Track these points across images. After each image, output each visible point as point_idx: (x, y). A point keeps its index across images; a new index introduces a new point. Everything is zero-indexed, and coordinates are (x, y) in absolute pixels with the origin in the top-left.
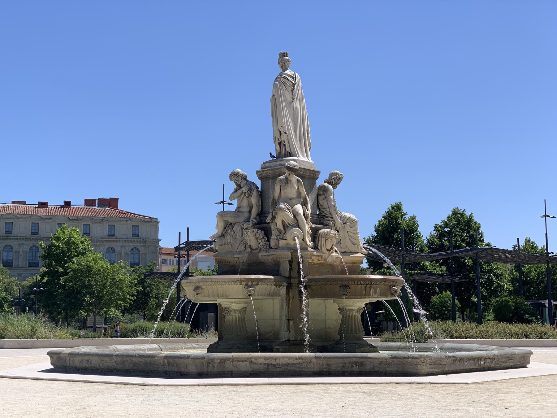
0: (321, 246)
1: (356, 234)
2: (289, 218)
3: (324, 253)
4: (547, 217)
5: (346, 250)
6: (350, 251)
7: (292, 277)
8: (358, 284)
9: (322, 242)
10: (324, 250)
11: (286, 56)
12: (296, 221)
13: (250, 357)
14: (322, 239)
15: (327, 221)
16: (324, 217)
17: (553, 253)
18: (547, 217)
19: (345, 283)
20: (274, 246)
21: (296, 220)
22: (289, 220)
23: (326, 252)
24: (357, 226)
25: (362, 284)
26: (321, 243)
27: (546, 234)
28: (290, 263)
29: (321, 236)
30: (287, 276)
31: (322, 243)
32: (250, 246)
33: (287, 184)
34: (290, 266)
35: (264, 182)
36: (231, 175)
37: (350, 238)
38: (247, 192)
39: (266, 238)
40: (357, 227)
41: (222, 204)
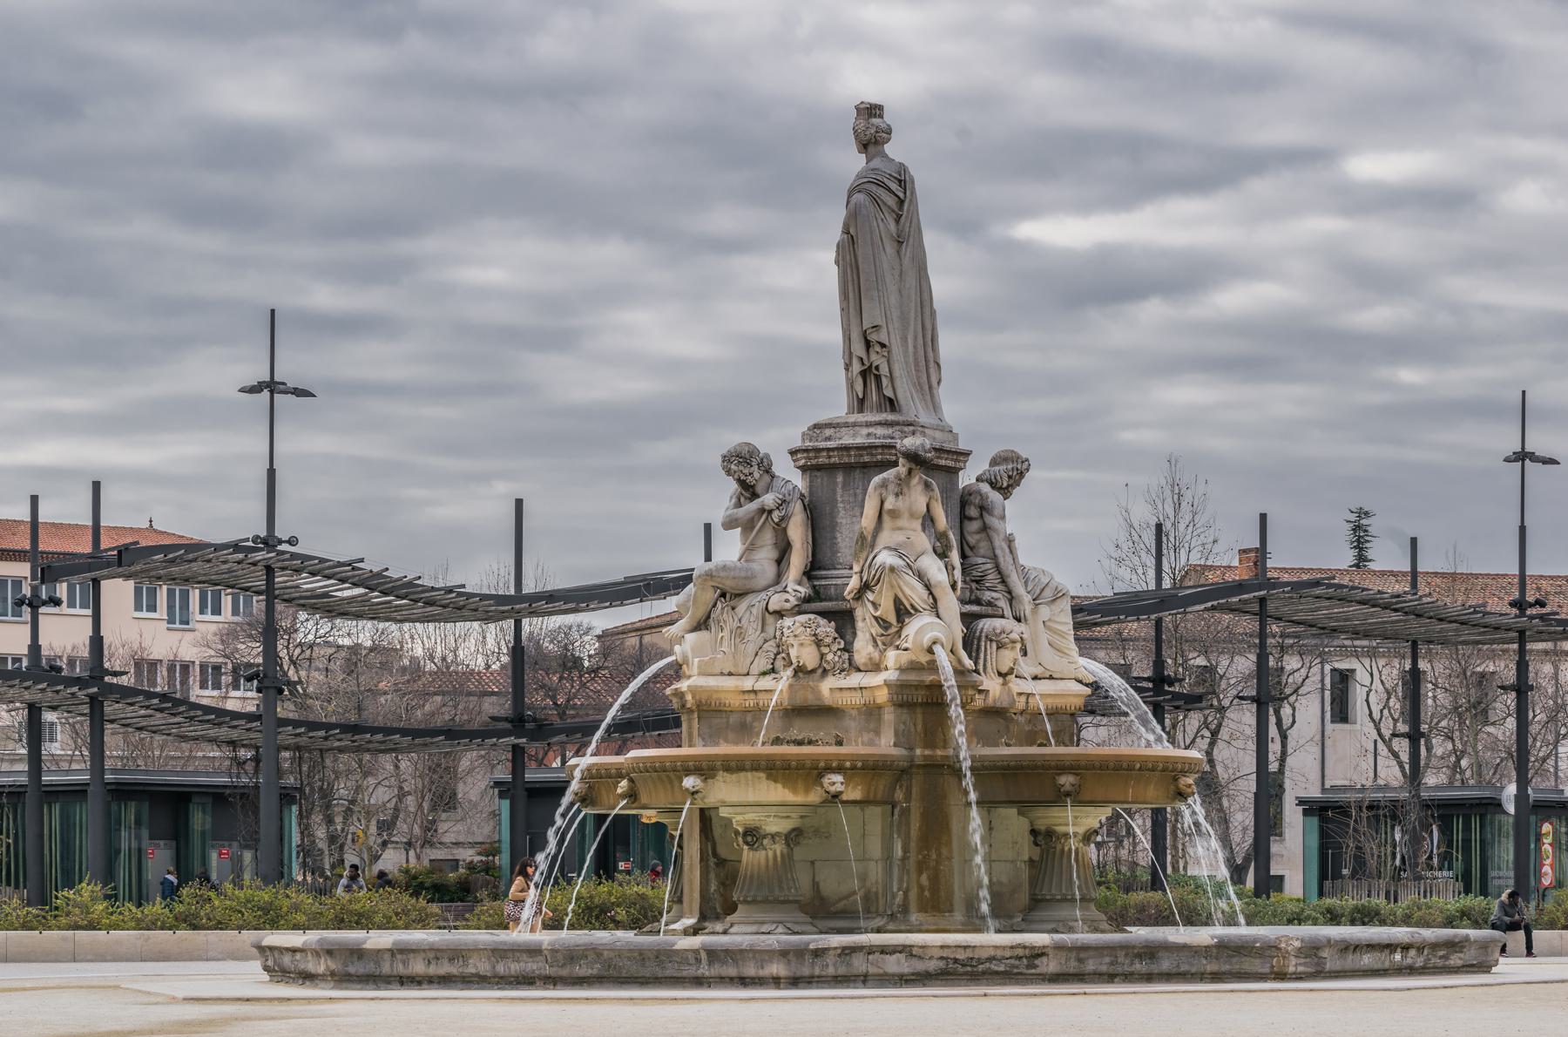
0: (985, 665)
4: (1527, 461)
9: (989, 652)
11: (875, 117)
12: (931, 600)
13: (908, 943)
14: (988, 647)
17: (1543, 605)
18: (1527, 461)
20: (865, 664)
27: (1523, 529)
29: (987, 637)
31: (989, 657)
33: (900, 497)
36: (727, 459)
39: (843, 643)
41: (266, 393)
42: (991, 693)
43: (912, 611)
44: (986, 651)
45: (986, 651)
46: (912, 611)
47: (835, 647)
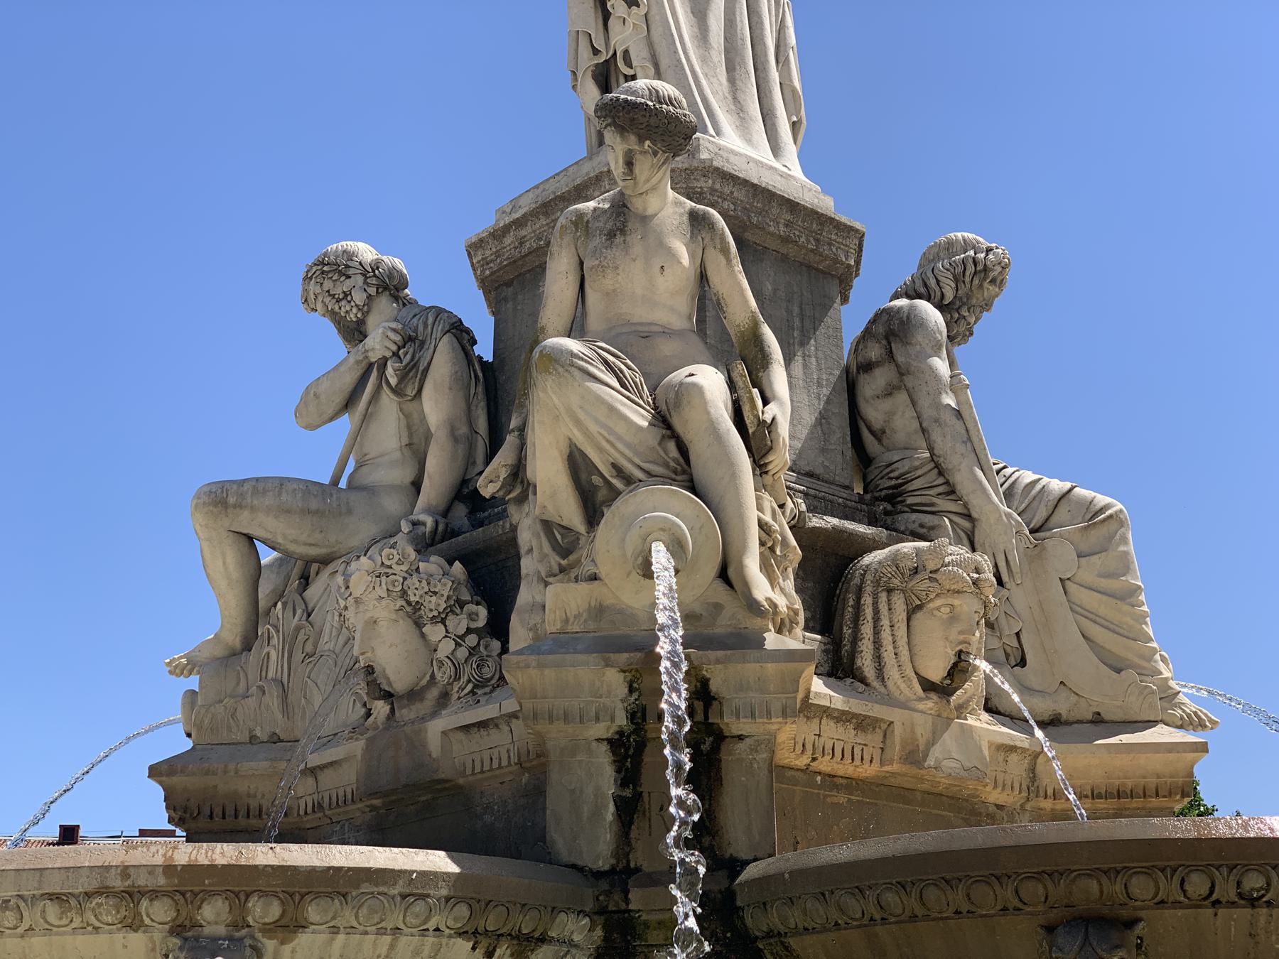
0: (878, 658)
1: (1122, 598)
2: (620, 429)
3: (904, 706)
5: (1063, 706)
6: (1090, 717)
7: (638, 870)
8: (1217, 903)
9: (885, 622)
10: (901, 682)
14: (883, 607)
15: (914, 516)
16: (901, 494)
19: (1089, 890)
21: (671, 446)
22: (620, 438)
23: (920, 699)
24: (1122, 548)
25: (1253, 902)
26: (877, 632)
28: (626, 756)
29: (877, 583)
30: (603, 864)
31: (886, 635)
32: (370, 670)
33: (619, 239)
34: (623, 784)
35: (510, 305)
37: (1087, 624)
38: (395, 354)
40: (1126, 554)
42: (898, 730)
43: (617, 483)
44: (876, 619)
45: (876, 619)
46: (617, 483)
47: (459, 624)
